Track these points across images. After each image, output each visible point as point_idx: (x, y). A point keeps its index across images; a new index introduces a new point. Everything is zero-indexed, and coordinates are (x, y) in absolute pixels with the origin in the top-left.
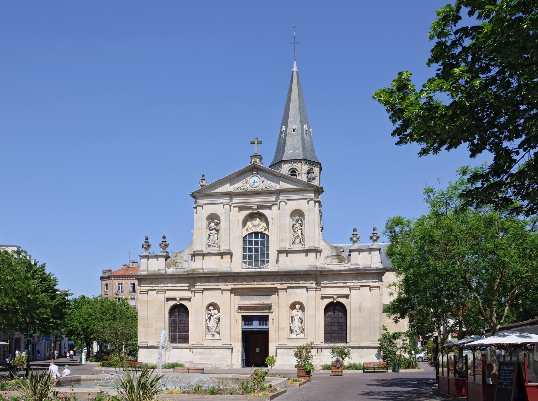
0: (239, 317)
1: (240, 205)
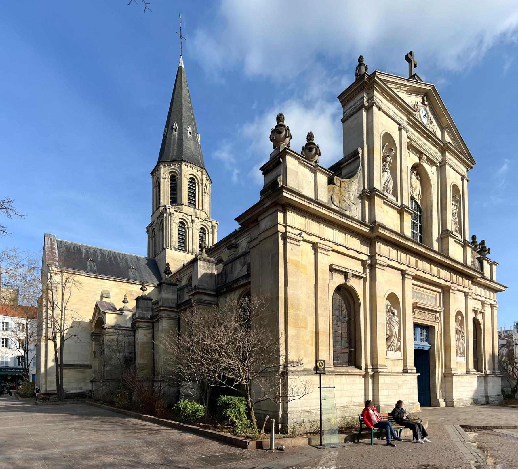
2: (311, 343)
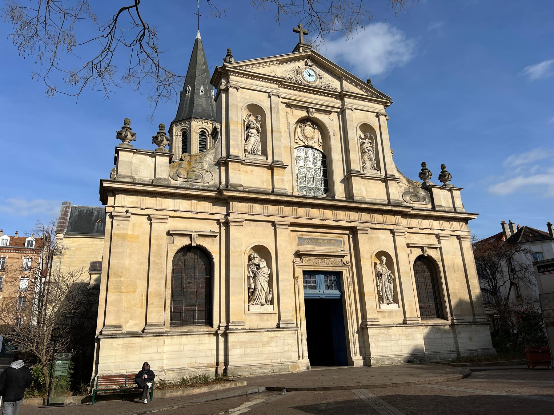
0: (299, 272)
1: (292, 102)
2: (140, 306)
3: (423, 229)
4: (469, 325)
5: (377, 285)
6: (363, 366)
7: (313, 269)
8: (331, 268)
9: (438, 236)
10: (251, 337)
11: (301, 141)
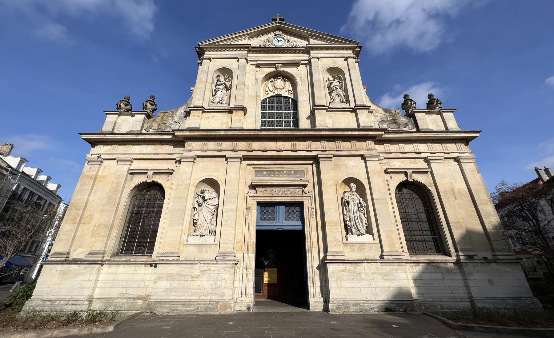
0: (253, 204)
2: (91, 235)
3: (405, 153)
4: (486, 264)
5: (343, 215)
6: (323, 310)
7: (268, 200)
8: (290, 198)
9: (426, 160)
10: (180, 269)
11: (272, 92)
